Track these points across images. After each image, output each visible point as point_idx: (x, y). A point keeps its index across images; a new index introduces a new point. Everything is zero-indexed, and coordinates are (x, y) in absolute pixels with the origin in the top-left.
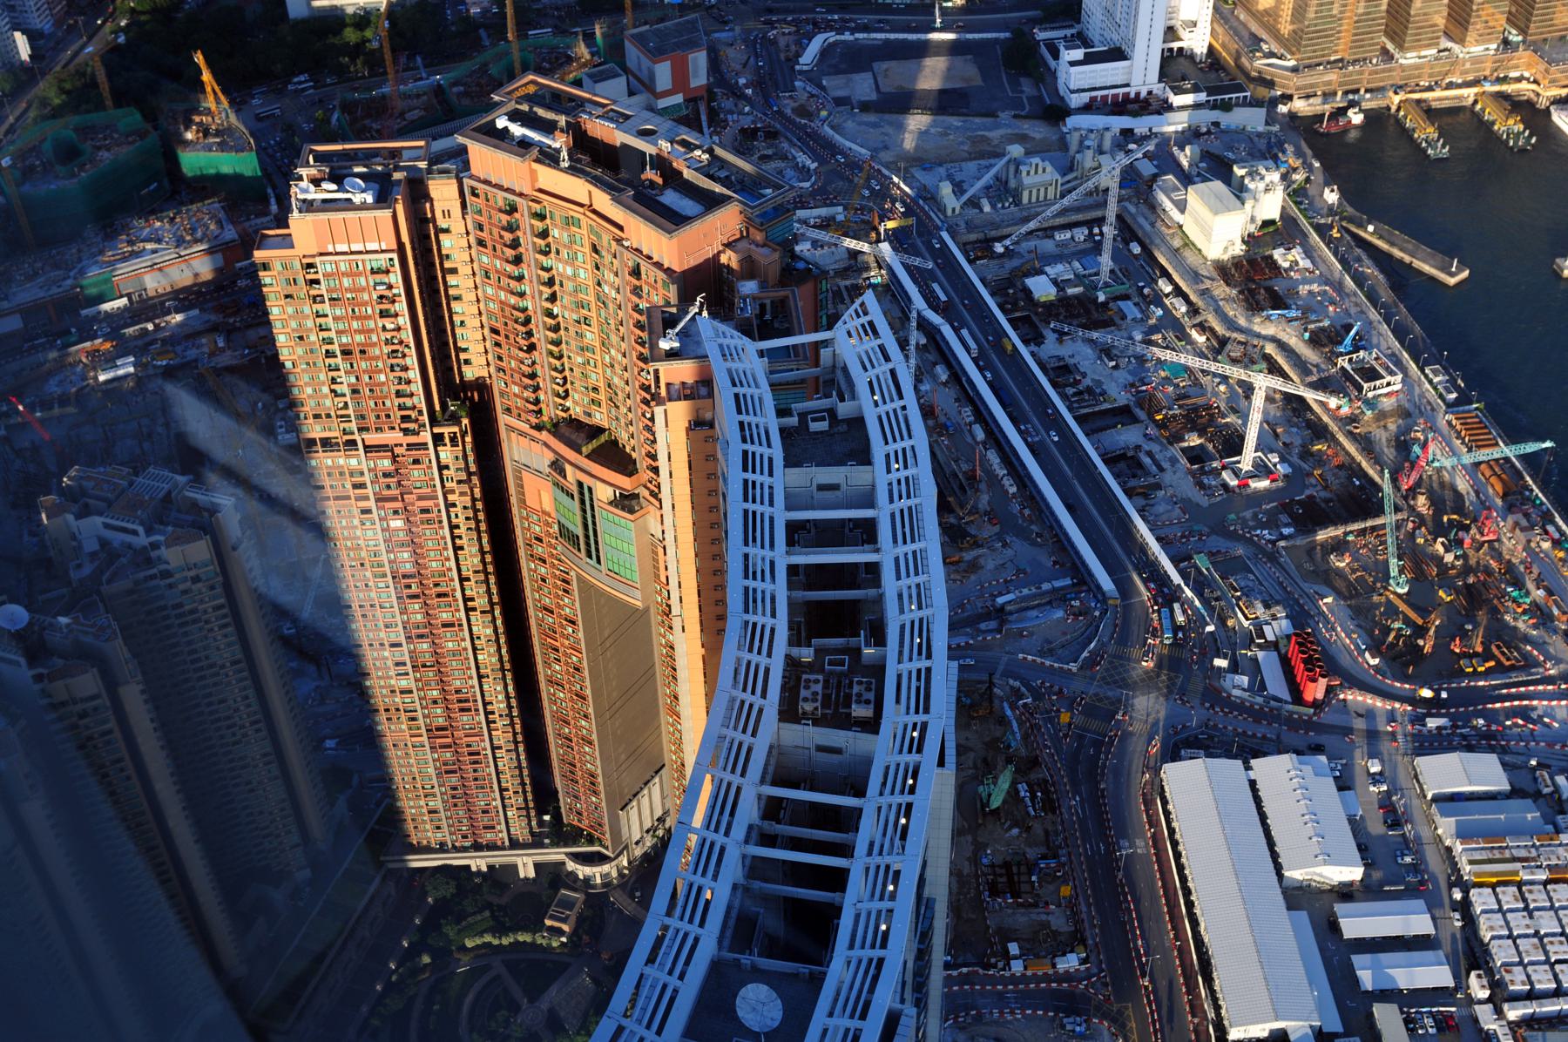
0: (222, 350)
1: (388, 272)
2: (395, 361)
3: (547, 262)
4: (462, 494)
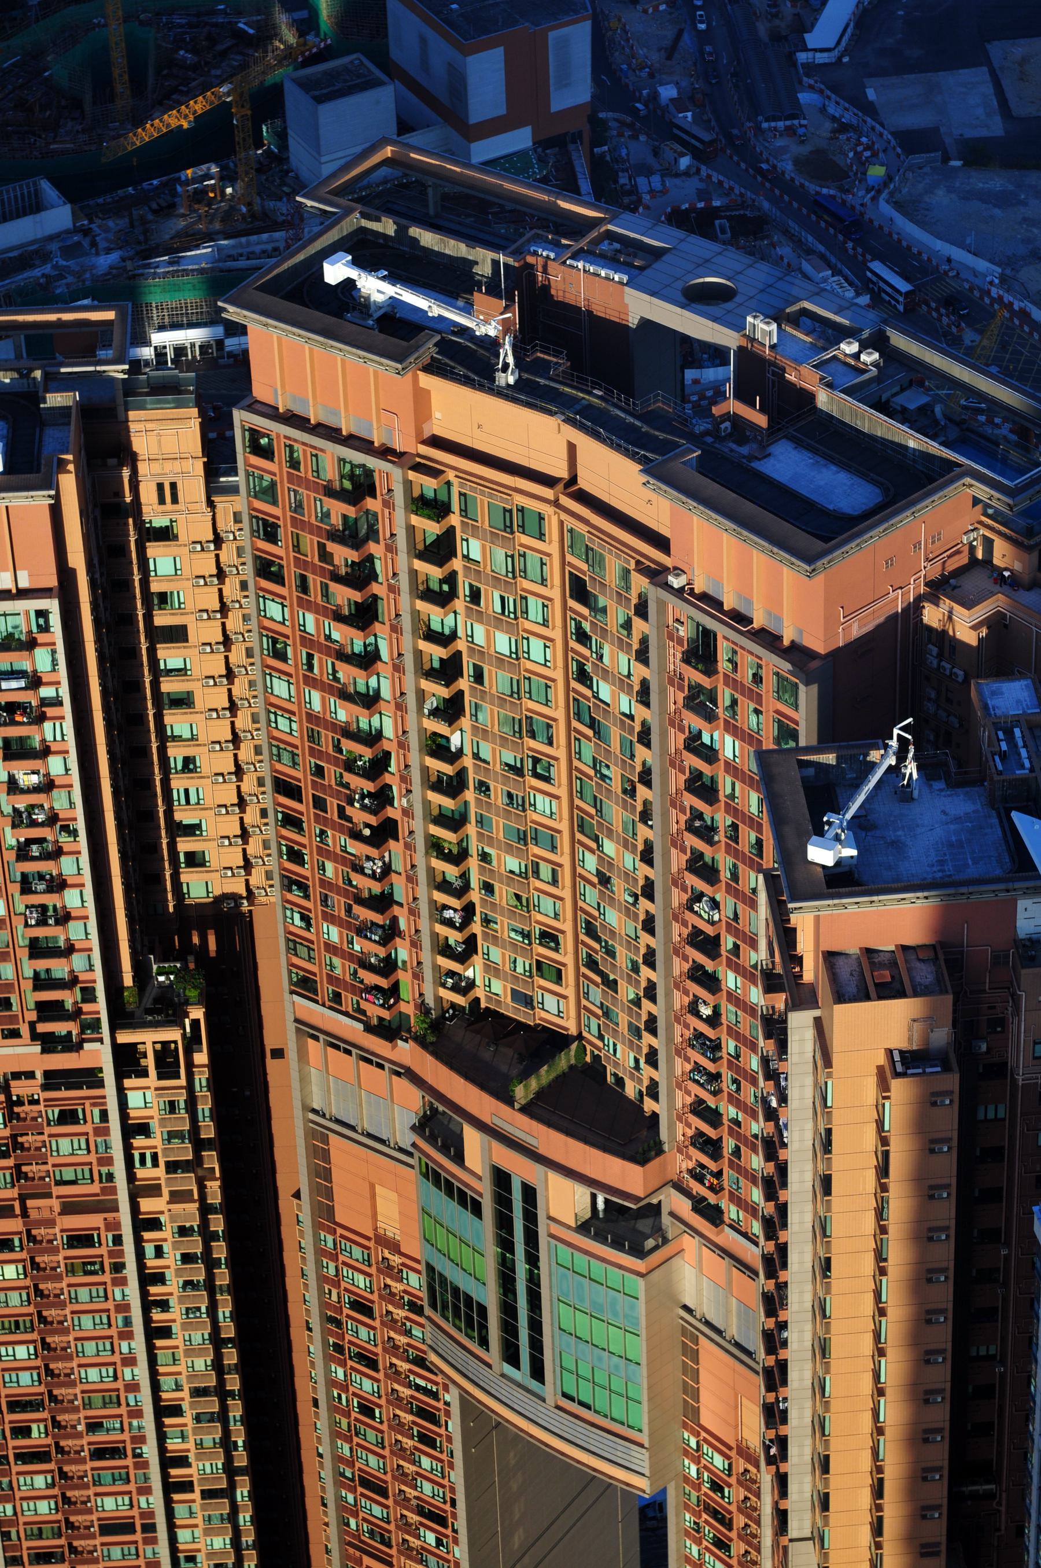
1: (31, 645)
2: (31, 867)
3: (437, 618)
4: (177, 1197)
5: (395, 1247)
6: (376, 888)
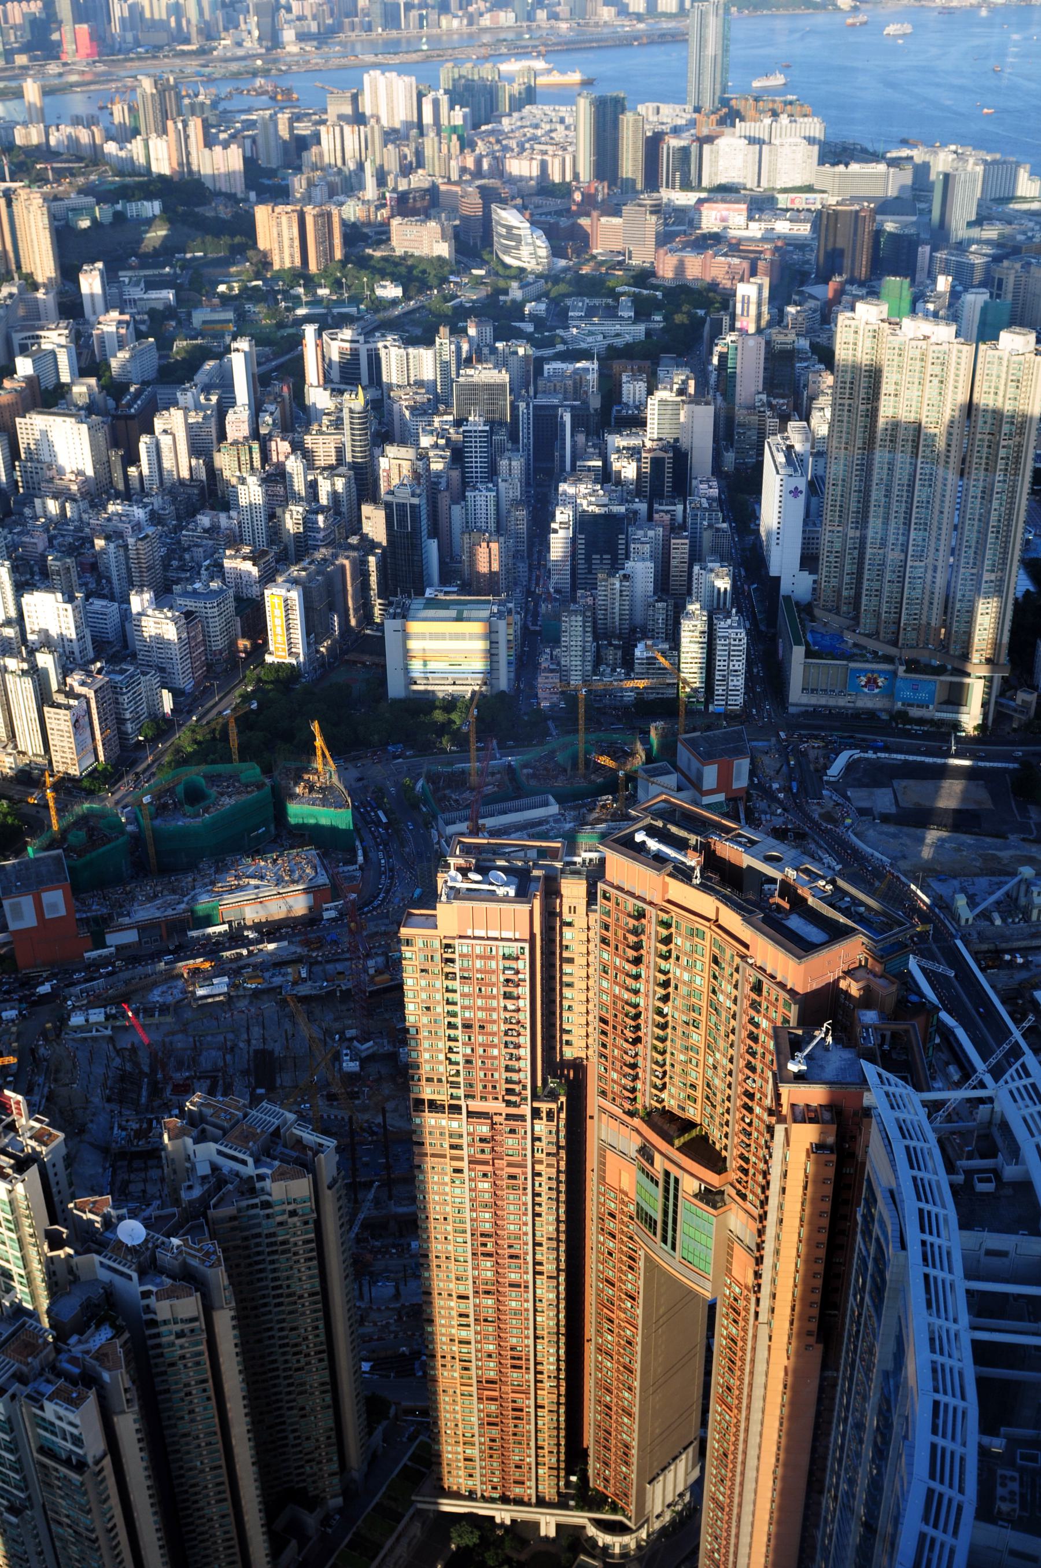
0: (304, 980)
1: (518, 958)
2: (509, 1039)
3: (664, 965)
4: (549, 1166)
5: (626, 1195)
6: (632, 1061)
